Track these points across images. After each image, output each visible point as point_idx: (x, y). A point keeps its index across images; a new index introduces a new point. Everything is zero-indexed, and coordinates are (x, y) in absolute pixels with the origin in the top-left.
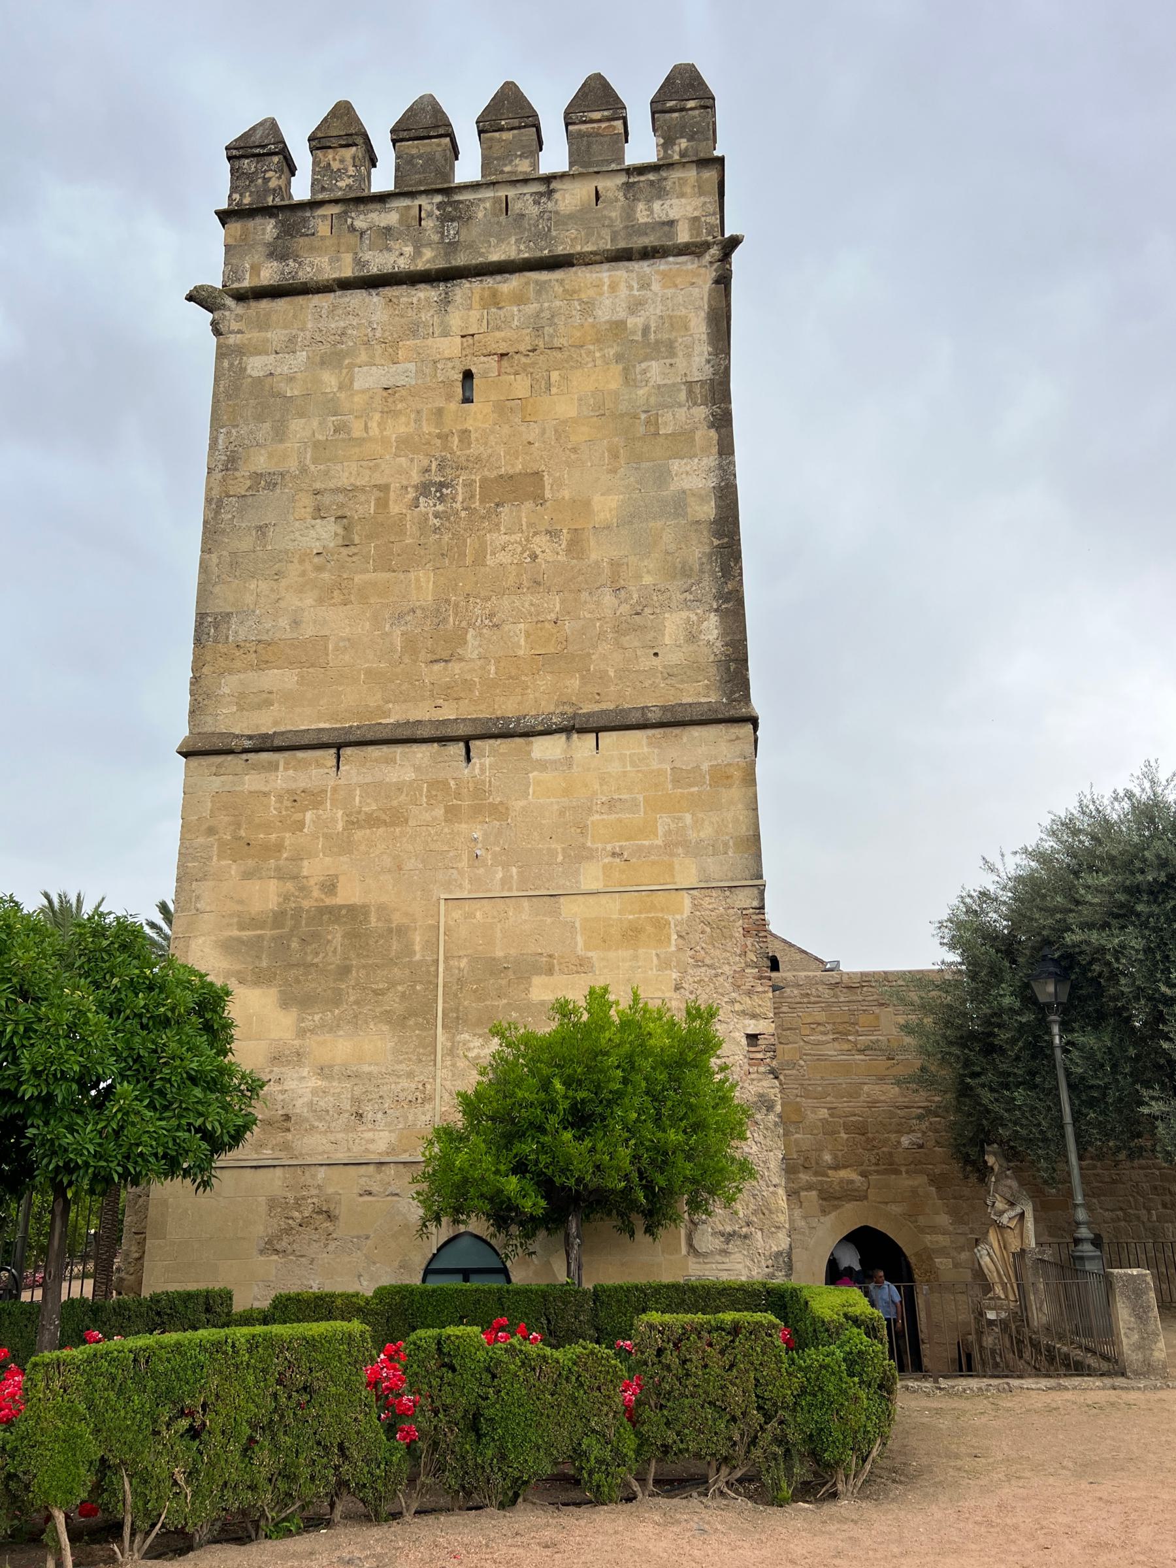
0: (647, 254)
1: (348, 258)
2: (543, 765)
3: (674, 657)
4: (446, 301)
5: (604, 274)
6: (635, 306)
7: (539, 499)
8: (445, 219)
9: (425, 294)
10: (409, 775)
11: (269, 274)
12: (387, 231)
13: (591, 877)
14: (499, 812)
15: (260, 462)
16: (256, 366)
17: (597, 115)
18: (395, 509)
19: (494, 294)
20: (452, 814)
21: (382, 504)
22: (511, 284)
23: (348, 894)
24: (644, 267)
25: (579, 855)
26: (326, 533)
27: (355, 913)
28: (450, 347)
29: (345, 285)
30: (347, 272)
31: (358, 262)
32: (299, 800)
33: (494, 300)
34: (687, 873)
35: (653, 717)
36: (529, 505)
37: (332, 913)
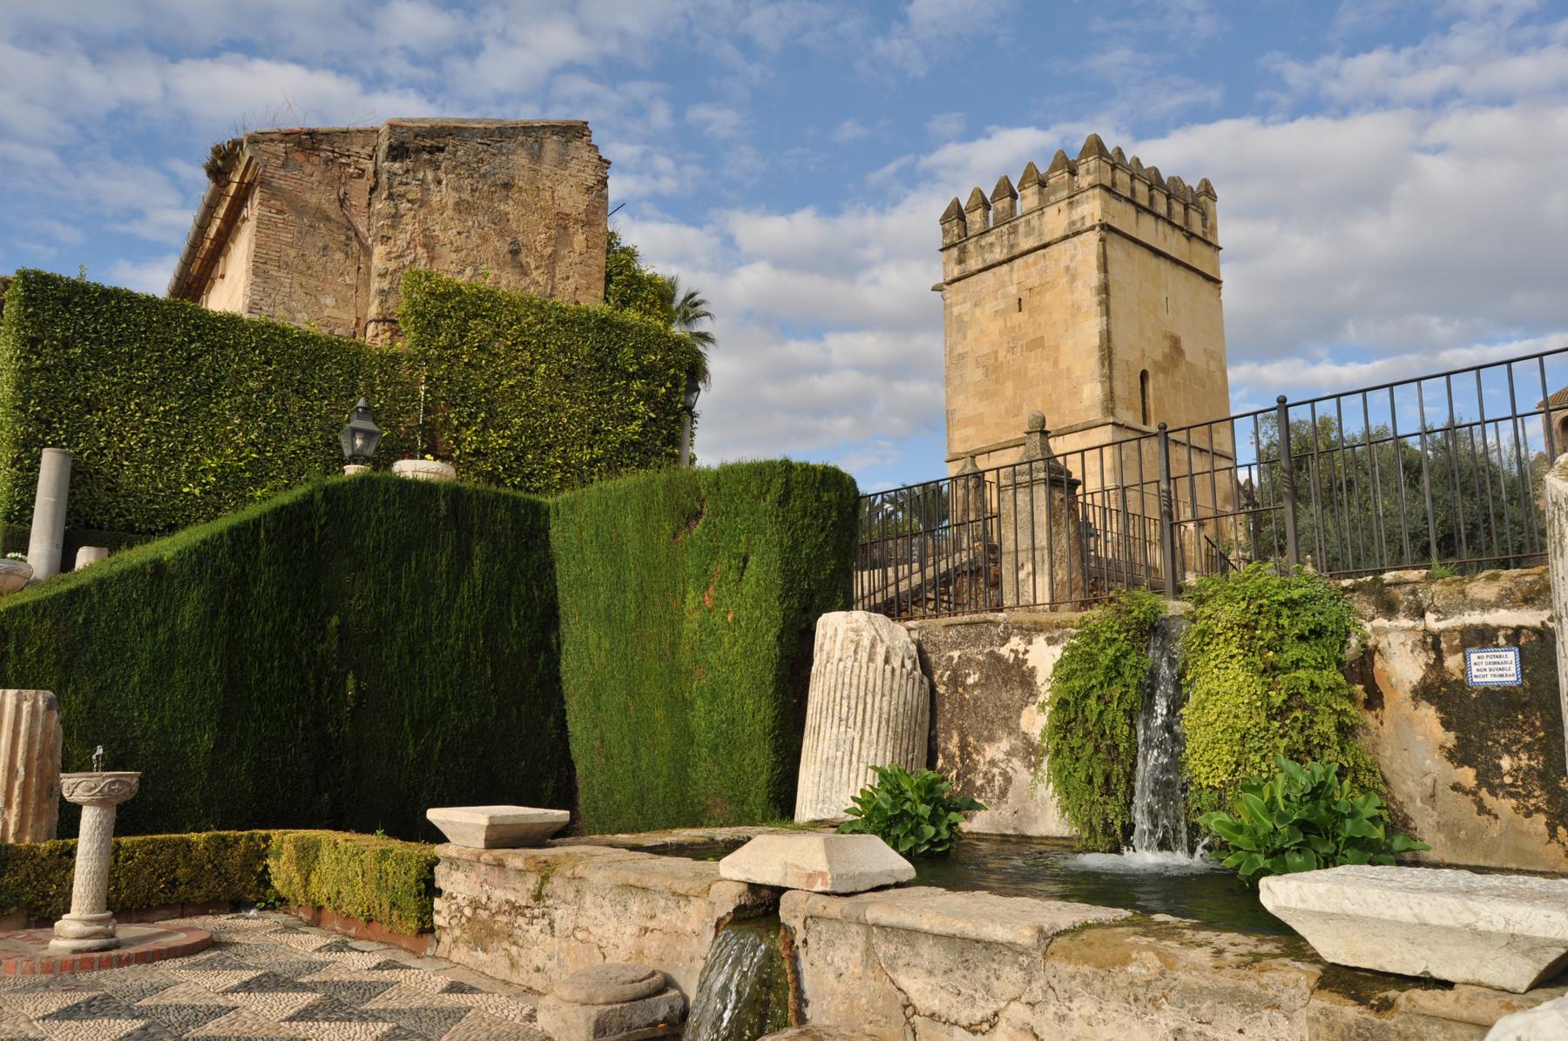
3: (1087, 403)
5: (1062, 245)
6: (1072, 258)
7: (1043, 346)
9: (1005, 268)
11: (956, 271)
12: (992, 244)
15: (959, 350)
16: (956, 311)
18: (1001, 359)
21: (996, 358)
22: (1031, 258)
24: (1075, 239)
26: (980, 372)
28: (1013, 290)
29: (980, 271)
33: (1027, 266)
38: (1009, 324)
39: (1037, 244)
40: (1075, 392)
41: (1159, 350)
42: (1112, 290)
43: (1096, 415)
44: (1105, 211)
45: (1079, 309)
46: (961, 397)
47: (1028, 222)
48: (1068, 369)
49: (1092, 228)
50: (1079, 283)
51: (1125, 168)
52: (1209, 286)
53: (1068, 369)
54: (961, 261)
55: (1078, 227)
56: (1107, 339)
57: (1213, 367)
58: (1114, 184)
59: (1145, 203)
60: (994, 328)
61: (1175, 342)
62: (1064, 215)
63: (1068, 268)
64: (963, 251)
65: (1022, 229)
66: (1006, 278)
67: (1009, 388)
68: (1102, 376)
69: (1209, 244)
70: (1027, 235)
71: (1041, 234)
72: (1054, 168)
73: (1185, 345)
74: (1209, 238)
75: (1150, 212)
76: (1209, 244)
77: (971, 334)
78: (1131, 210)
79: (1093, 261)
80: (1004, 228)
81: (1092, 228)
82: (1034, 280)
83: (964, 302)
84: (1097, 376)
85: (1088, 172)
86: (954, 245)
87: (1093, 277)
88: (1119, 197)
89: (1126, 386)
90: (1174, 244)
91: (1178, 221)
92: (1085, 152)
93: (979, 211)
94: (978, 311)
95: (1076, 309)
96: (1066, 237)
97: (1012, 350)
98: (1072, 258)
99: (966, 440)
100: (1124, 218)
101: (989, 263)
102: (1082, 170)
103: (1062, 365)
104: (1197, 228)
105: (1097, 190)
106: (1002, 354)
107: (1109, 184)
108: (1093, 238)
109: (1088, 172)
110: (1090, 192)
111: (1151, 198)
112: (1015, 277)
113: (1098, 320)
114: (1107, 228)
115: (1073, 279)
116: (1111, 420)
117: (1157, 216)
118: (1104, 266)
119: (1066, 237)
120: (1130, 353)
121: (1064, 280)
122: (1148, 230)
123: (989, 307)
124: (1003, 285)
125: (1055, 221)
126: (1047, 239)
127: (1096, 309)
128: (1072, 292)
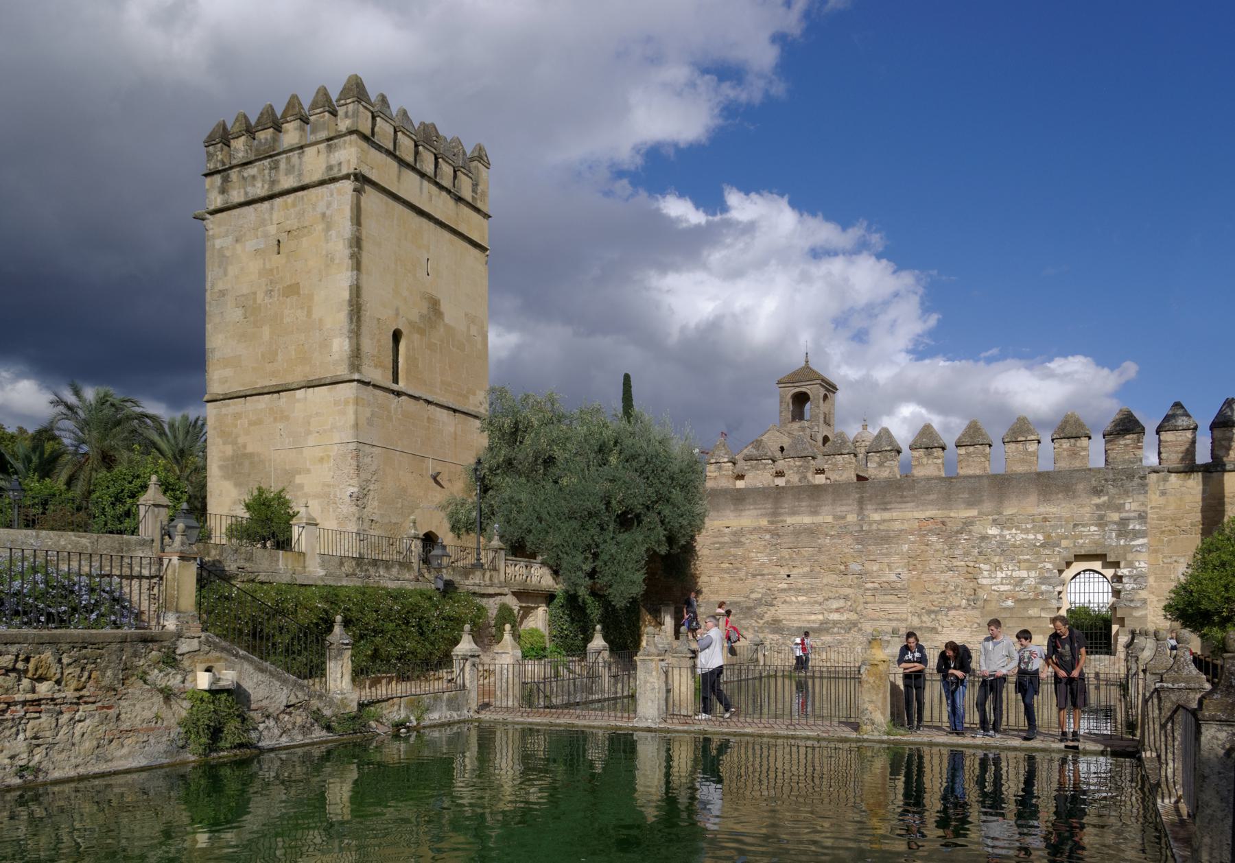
0: (333, 180)
1: (242, 191)
2: (298, 401)
3: (336, 357)
4: (272, 209)
5: (320, 190)
6: (329, 205)
7: (298, 294)
8: (271, 169)
10: (264, 406)
12: (254, 177)
13: (311, 440)
14: (287, 418)
17: (318, 111)
19: (286, 202)
20: (275, 419)
21: (255, 300)
22: (290, 198)
23: (250, 449)
24: (332, 186)
25: (308, 433)
26: (240, 312)
27: (251, 455)
28: (272, 229)
29: (241, 205)
30: (242, 199)
31: (246, 193)
32: (237, 416)
34: (337, 437)
35: (328, 381)
36: (295, 297)
37: (245, 455)
38: (268, 266)
39: (296, 185)
40: (325, 345)
41: (414, 311)
42: (365, 244)
43: (343, 371)
44: (361, 160)
45: (332, 260)
46: (221, 336)
47: (288, 159)
48: (320, 320)
49: (347, 177)
50: (333, 233)
51: (388, 118)
52: (476, 252)
53: (320, 320)
54: (223, 191)
55: (335, 173)
56: (356, 291)
57: (474, 331)
58: (373, 133)
59: (410, 158)
60: (254, 266)
61: (434, 304)
62: (323, 157)
63: (324, 215)
64: (226, 180)
65: (283, 165)
66: (267, 216)
67: (266, 331)
68: (351, 331)
69: (478, 210)
70: (289, 172)
71: (300, 175)
72: (314, 105)
73: (445, 307)
74: (479, 205)
75: (414, 169)
76: (478, 210)
77: (232, 270)
78: (395, 164)
79: (347, 212)
80: (266, 162)
81: (347, 177)
82: (292, 223)
83: (226, 235)
84: (345, 331)
85: (346, 115)
86: (218, 172)
87: (345, 227)
88: (379, 148)
89: (375, 344)
90: (441, 206)
91: (447, 183)
92: (345, 93)
93: (243, 139)
94: (238, 246)
95: (329, 259)
96: (322, 183)
97: (269, 293)
98: (329, 205)
99: (224, 381)
100: (383, 169)
101: (250, 197)
102: (341, 111)
103: (315, 316)
104: (467, 194)
105: (354, 137)
106: (260, 295)
107: (368, 132)
108: (348, 185)
109: (346, 115)
110: (348, 138)
111: (417, 153)
112: (275, 216)
113: (349, 274)
114: (362, 180)
115: (328, 228)
116: (356, 377)
117: (423, 175)
118: (357, 219)
119: (322, 183)
120: (383, 309)
121: (320, 227)
122: (410, 186)
123: (251, 244)
124: (263, 223)
125: (314, 163)
126: (306, 181)
127: (348, 262)
128: (327, 241)
